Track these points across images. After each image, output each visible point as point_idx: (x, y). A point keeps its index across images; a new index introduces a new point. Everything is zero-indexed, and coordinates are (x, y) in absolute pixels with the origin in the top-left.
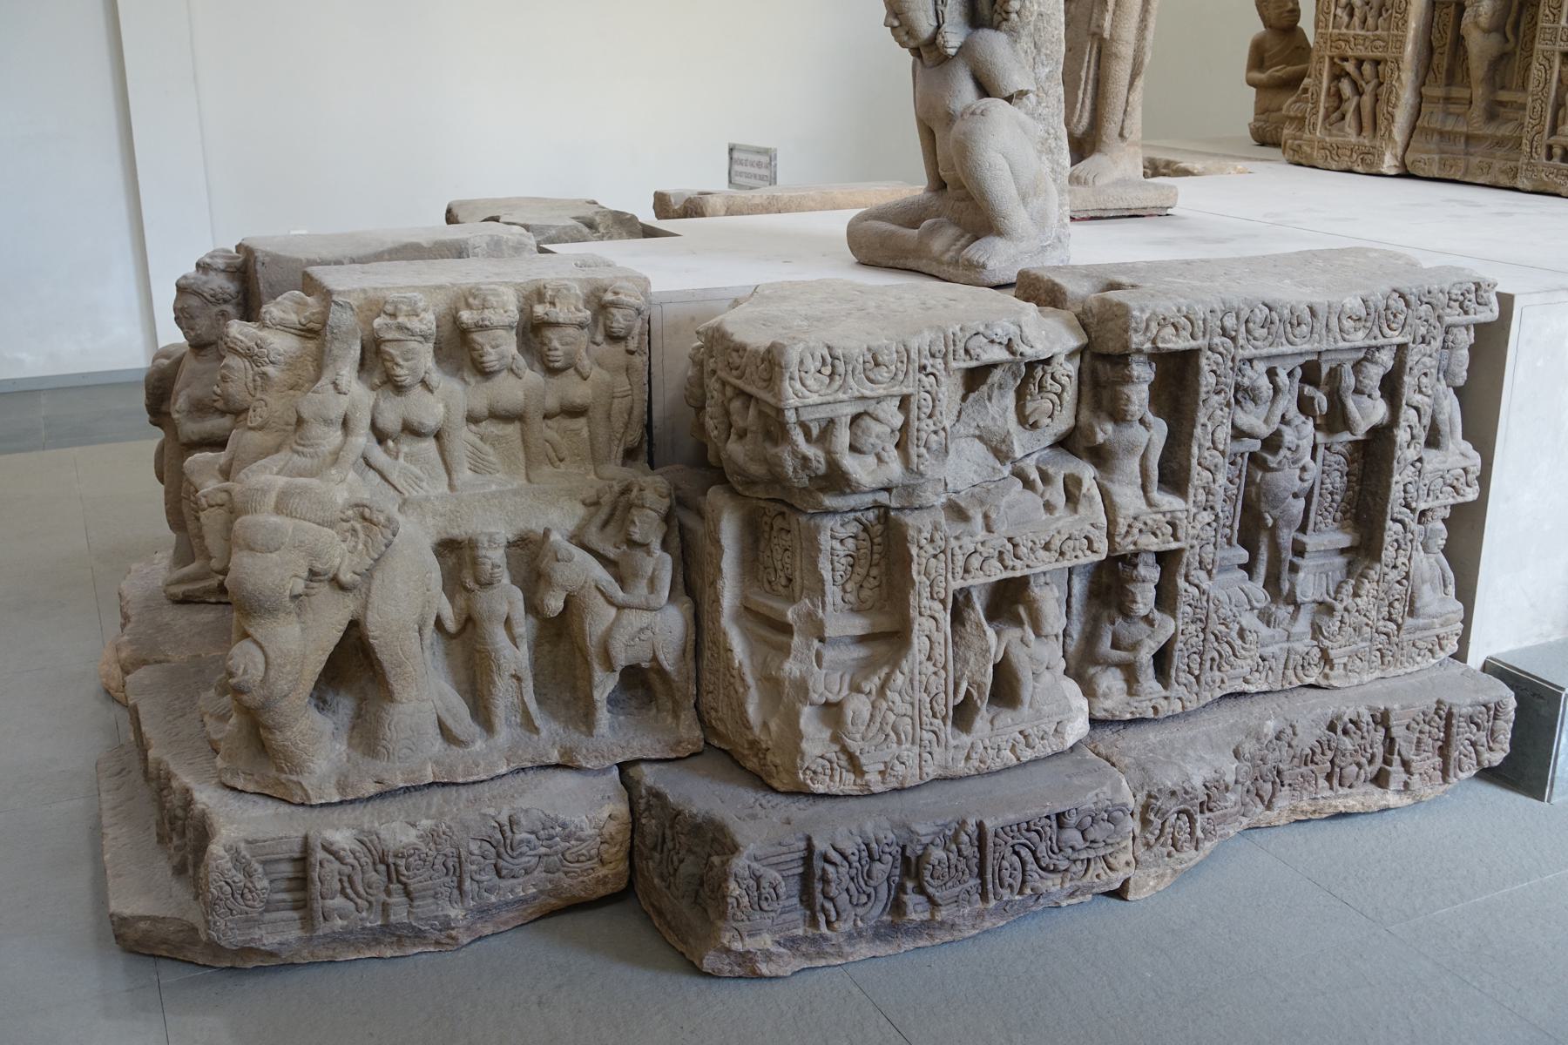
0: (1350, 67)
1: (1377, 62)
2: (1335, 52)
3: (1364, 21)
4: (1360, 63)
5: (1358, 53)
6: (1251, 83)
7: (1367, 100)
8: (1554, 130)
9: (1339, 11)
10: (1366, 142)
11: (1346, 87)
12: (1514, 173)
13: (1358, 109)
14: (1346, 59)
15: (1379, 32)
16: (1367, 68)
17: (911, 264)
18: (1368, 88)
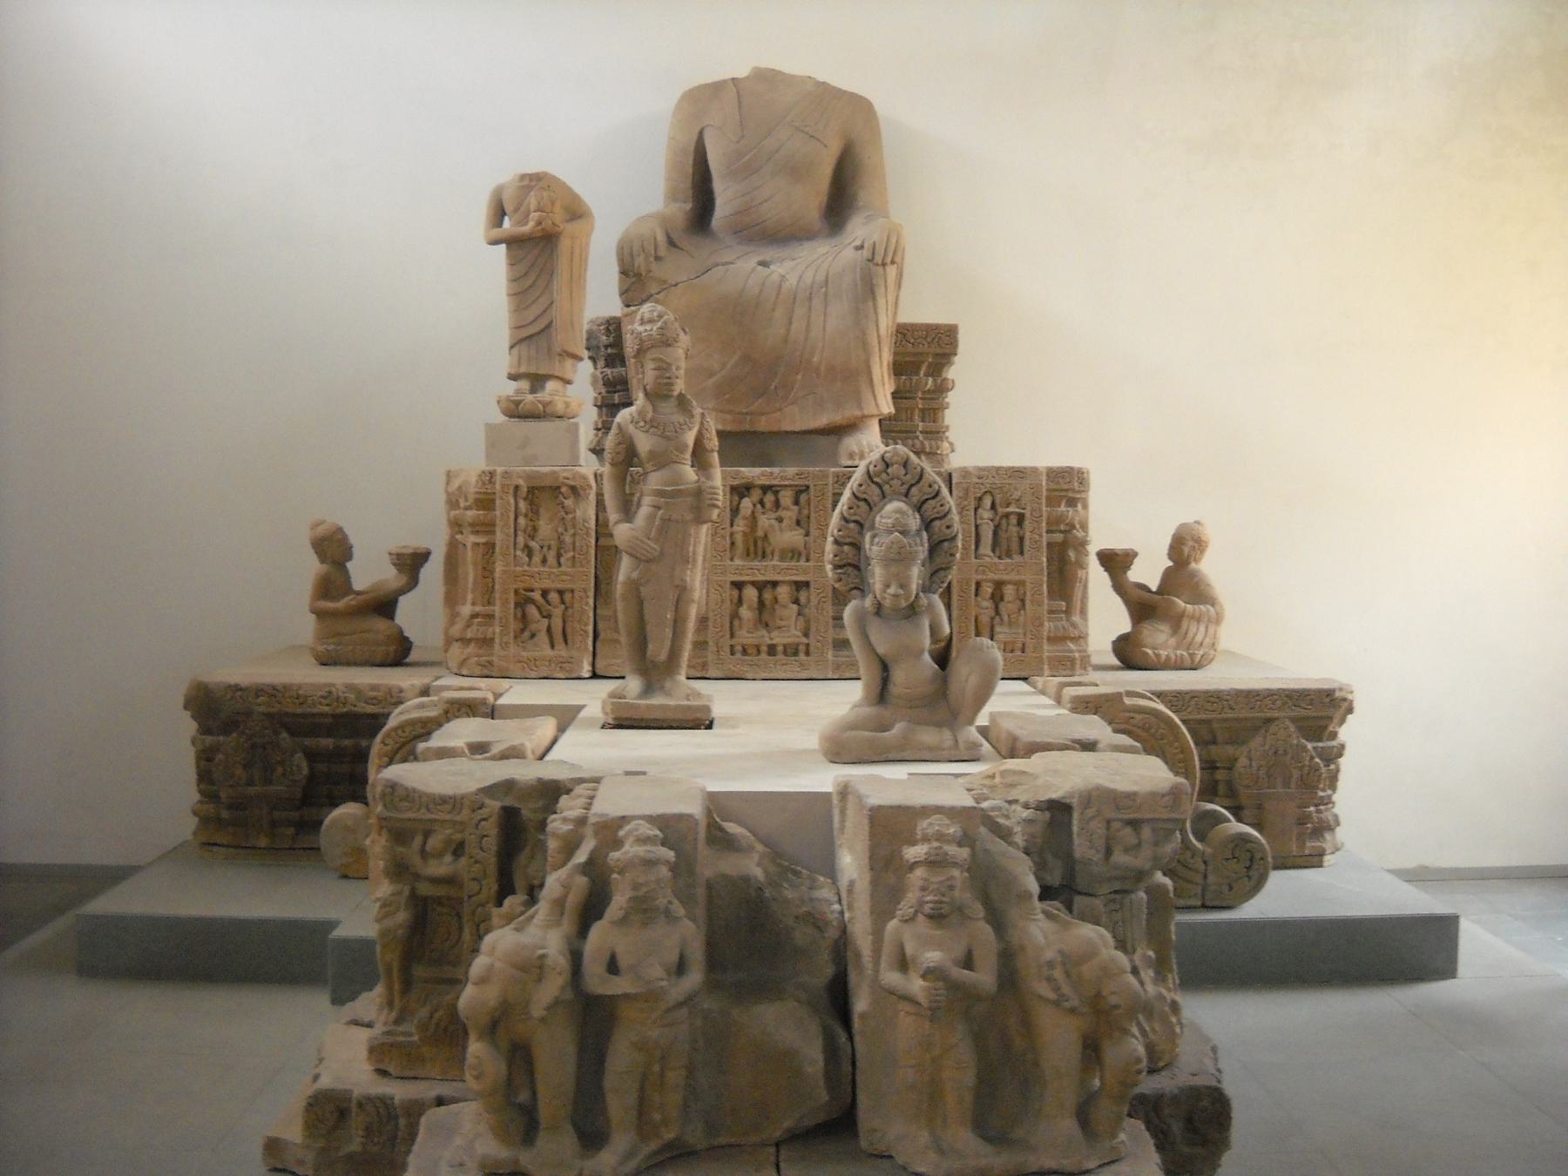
0: (537, 596)
1: (561, 592)
2: (522, 585)
3: (544, 561)
4: (545, 593)
5: (547, 584)
6: (314, 611)
7: (557, 623)
8: (732, 636)
9: (519, 553)
10: (563, 653)
11: (532, 611)
12: (704, 666)
13: (549, 630)
14: (532, 591)
15: (563, 569)
16: (553, 596)
17: (891, 756)
18: (557, 612)
